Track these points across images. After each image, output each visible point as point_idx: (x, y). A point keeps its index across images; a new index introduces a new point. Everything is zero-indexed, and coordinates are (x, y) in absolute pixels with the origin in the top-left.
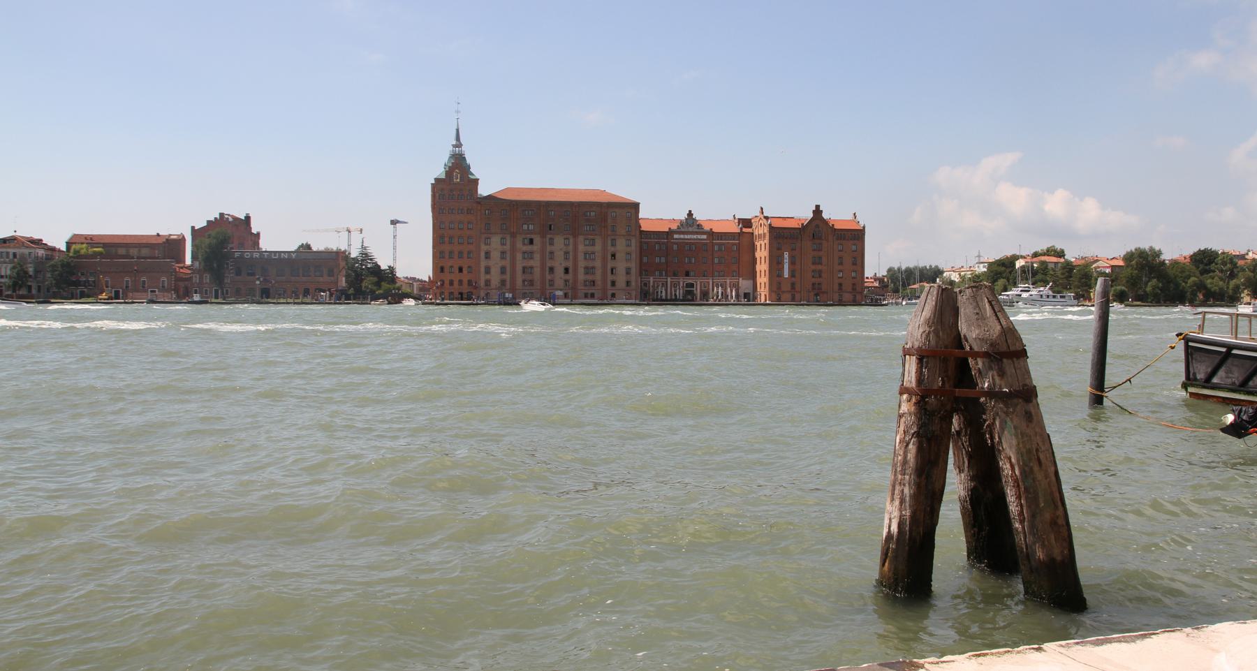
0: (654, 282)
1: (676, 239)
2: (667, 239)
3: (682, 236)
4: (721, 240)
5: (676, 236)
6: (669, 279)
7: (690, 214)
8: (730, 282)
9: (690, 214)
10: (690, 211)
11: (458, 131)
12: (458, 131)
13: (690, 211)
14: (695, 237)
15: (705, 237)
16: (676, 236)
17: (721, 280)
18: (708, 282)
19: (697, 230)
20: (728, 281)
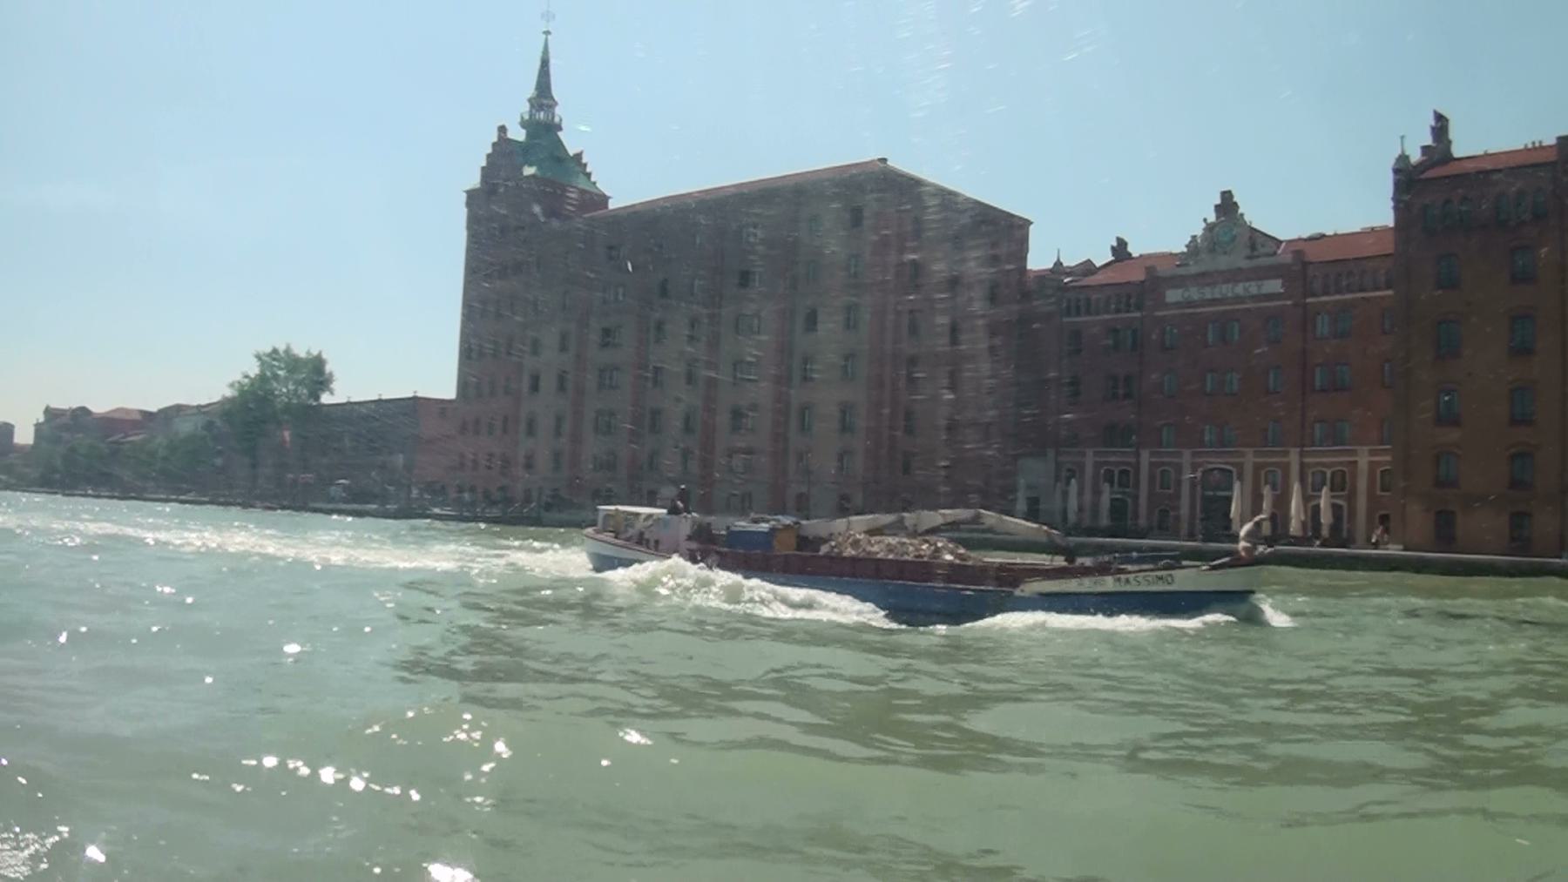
0: (1097, 465)
1: (1178, 305)
2: (1139, 308)
3: (1194, 293)
4: (1339, 292)
5: (1173, 295)
6: (1145, 456)
7: (1227, 205)
8: (1371, 463)
9: (1227, 205)
10: (1227, 196)
11: (545, 63)
12: (545, 63)
13: (1227, 196)
14: (1239, 289)
15: (1274, 286)
16: (1173, 295)
17: (1328, 459)
18: (1286, 468)
19: (1244, 264)
20: (1363, 461)
